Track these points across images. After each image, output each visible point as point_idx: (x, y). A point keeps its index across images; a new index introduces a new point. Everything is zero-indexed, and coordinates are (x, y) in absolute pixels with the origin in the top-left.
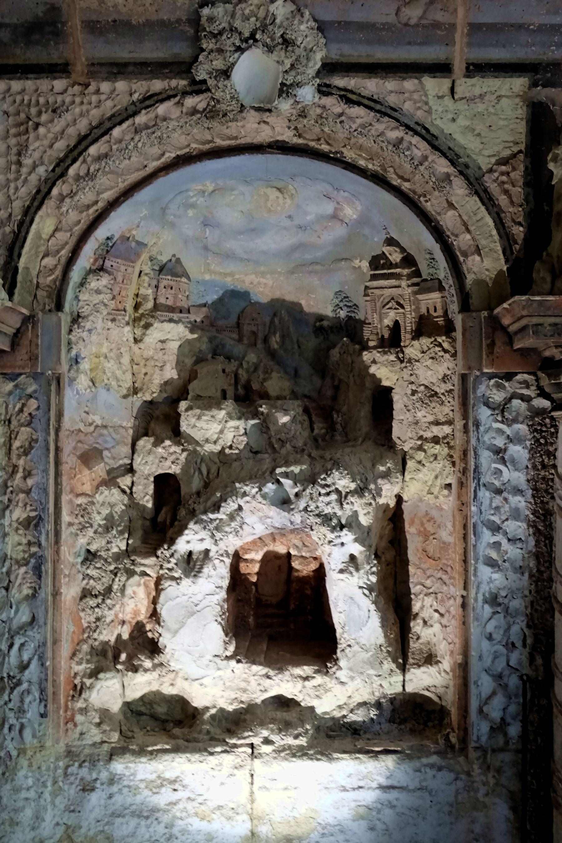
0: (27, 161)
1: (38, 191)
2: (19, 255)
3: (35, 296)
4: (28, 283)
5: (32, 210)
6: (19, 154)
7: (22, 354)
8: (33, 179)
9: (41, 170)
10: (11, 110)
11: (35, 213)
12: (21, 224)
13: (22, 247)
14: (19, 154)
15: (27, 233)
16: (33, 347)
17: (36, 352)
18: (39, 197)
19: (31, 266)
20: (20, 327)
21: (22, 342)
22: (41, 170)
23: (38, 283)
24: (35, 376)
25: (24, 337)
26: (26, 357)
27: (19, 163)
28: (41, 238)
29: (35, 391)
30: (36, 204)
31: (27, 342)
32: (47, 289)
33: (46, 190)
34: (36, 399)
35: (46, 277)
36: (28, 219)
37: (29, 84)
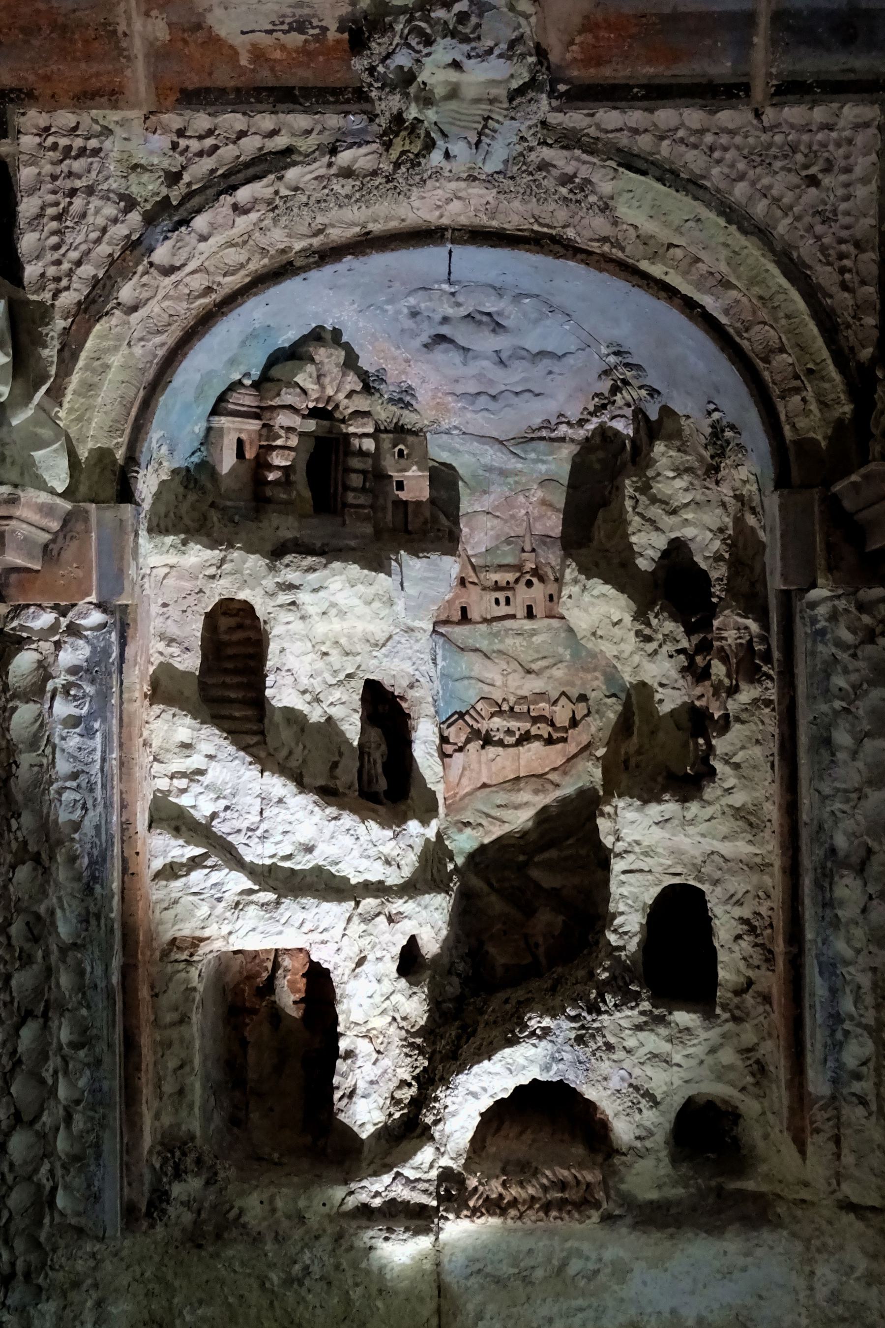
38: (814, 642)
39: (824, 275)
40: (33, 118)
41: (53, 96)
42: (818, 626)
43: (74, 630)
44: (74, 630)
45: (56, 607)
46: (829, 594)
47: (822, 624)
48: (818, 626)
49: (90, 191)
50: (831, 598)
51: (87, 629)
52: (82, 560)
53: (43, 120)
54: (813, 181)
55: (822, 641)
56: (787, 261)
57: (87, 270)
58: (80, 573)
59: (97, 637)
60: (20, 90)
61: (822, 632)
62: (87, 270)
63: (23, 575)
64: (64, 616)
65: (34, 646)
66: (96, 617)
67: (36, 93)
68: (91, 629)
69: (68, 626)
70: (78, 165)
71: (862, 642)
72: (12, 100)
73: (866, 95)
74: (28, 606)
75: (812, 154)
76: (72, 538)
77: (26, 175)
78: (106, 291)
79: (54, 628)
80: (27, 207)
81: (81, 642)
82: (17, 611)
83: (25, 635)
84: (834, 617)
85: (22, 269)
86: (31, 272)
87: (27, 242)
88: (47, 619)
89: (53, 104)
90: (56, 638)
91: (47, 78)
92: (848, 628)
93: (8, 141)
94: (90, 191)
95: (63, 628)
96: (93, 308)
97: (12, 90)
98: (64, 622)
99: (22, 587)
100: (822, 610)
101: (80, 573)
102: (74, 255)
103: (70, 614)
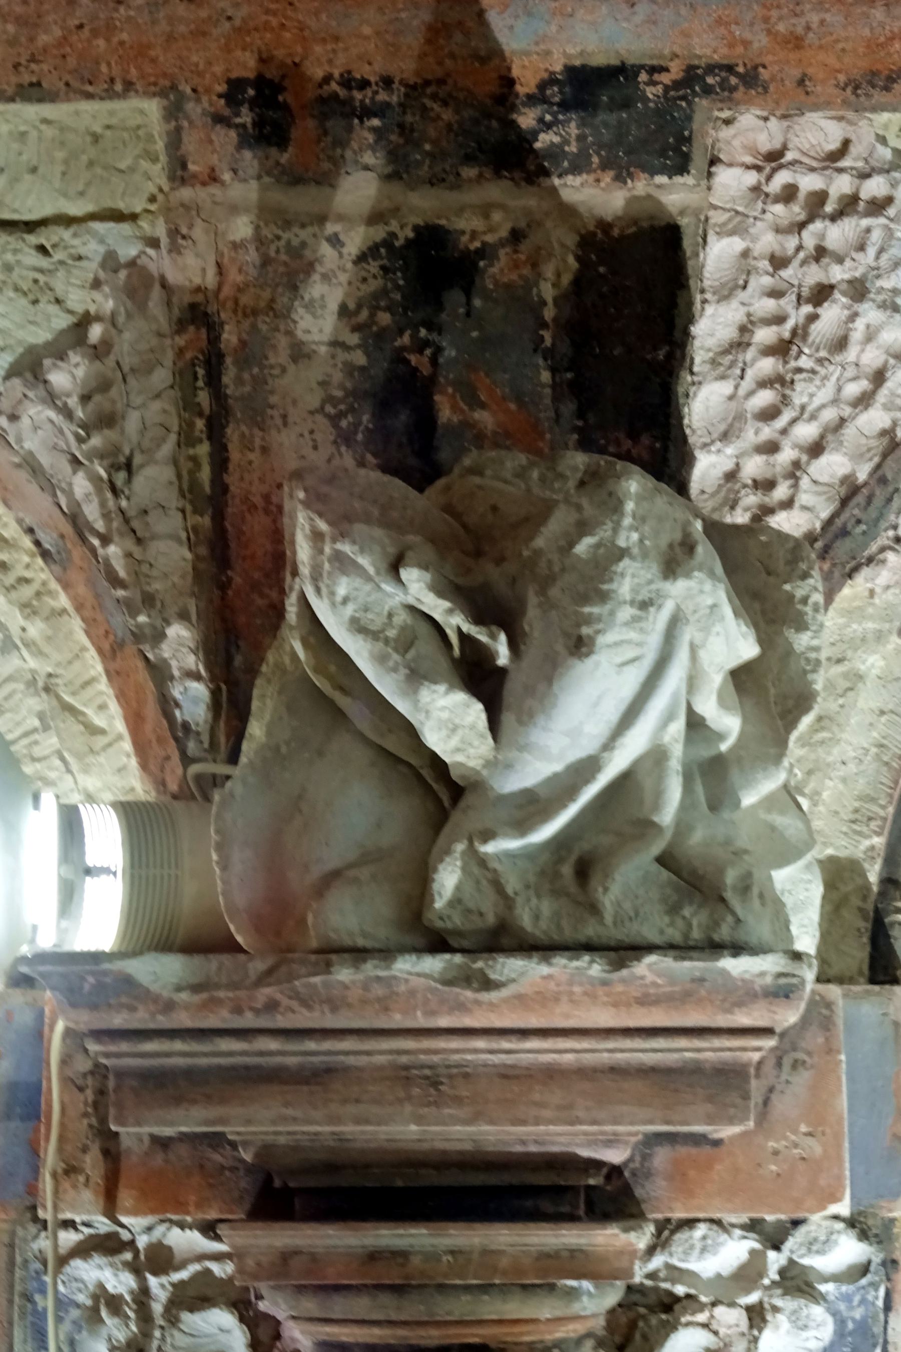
40: (747, 130)
41: (801, 82)
43: (797, 1283)
44: (797, 1283)
45: (753, 1226)
49: (858, 290)
51: (826, 1279)
52: (818, 1116)
53: (766, 141)
57: (833, 465)
58: (815, 1147)
59: (847, 1298)
60: (730, 69)
62: (833, 465)
63: (683, 1150)
64: (777, 1248)
65: (702, 1317)
66: (849, 1250)
67: (764, 74)
68: (836, 1278)
69: (782, 1272)
70: (837, 234)
72: (708, 91)
74: (690, 1223)
76: (795, 1065)
77: (716, 256)
78: (873, 512)
79: (748, 1274)
80: (712, 326)
81: (817, 1311)
82: (667, 1232)
83: (680, 1290)
85: (687, 459)
86: (707, 468)
87: (705, 402)
88: (734, 1251)
89: (801, 96)
90: (753, 1298)
91: (796, 42)
93: (689, 180)
94: (858, 290)
95: (773, 1274)
96: (842, 548)
97: (711, 69)
98: (775, 1260)
99: (679, 1177)
101: (815, 1147)
102: (806, 432)
103: (790, 1244)
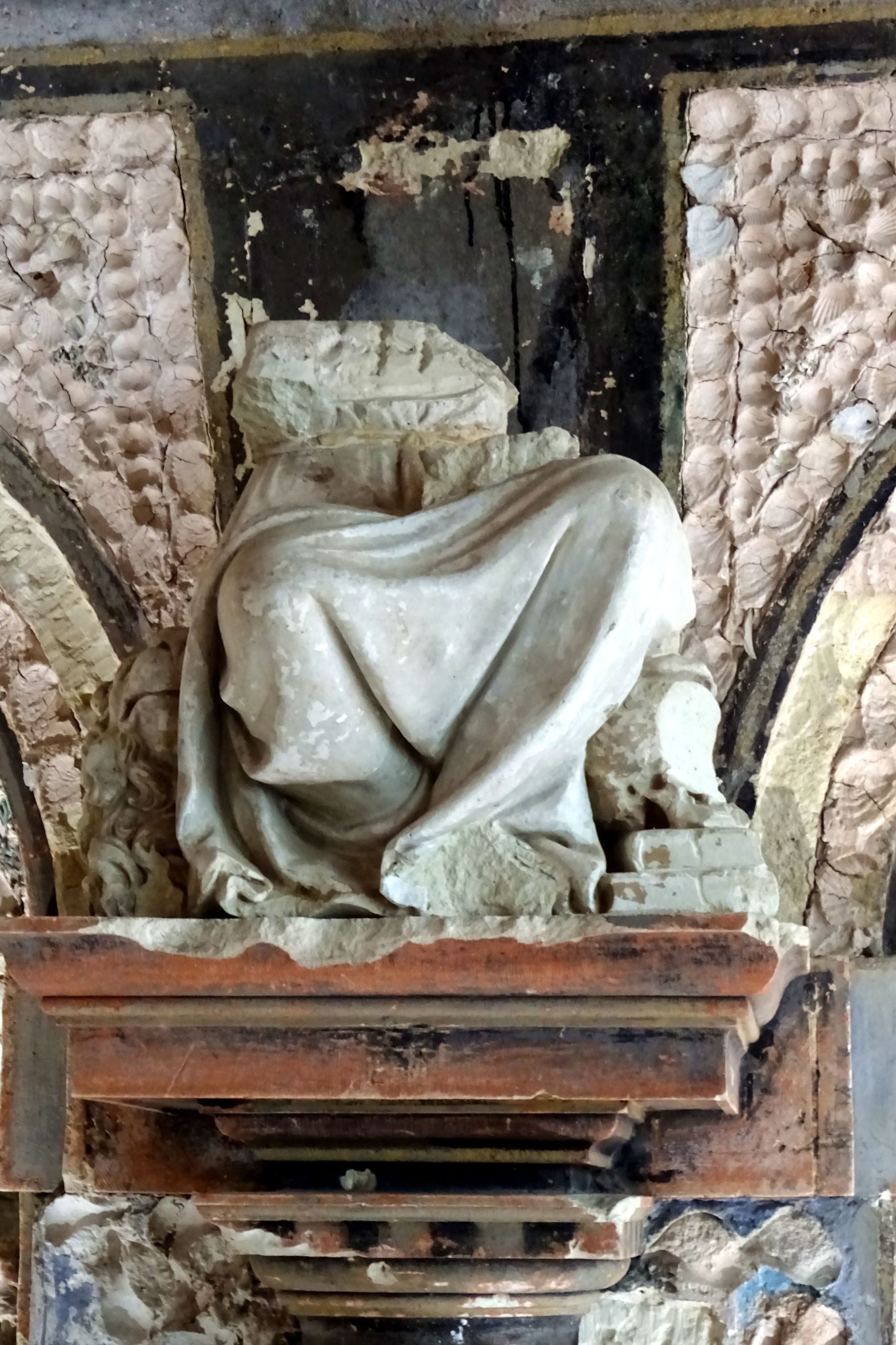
0: (801, 391)
1: (838, 502)
2: (761, 744)
3: (815, 891)
4: (788, 849)
5: (813, 573)
6: (772, 364)
7: (783, 1124)
8: (820, 454)
9: (852, 424)
10: (751, 201)
11: (824, 583)
12: (768, 624)
13: (772, 710)
14: (772, 364)
15: (791, 658)
16: (828, 1100)
17: (838, 1116)
18: (841, 523)
19: (798, 784)
20: (775, 1022)
21: (780, 1078)
22: (852, 424)
23: (823, 846)
24: (830, 1212)
25: (790, 1056)
26: (799, 1138)
27: (771, 399)
28: (835, 678)
29: (831, 1274)
30: (827, 548)
31: (806, 1080)
32: (857, 868)
33: (868, 496)
34: (836, 1302)
35: (856, 824)
36: (795, 606)
37: (826, 102)
38: (63, 1317)
39: (103, 493)
42: (72, 1283)
46: (97, 1209)
47: (79, 1279)
48: (72, 1283)
50: (100, 1220)
54: (46, 284)
55: (80, 1319)
56: (14, 460)
61: (78, 1299)
71: (167, 1326)
73: (133, 97)
75: (37, 228)
84: (108, 1263)
92: (139, 1290)
100: (81, 1246)
